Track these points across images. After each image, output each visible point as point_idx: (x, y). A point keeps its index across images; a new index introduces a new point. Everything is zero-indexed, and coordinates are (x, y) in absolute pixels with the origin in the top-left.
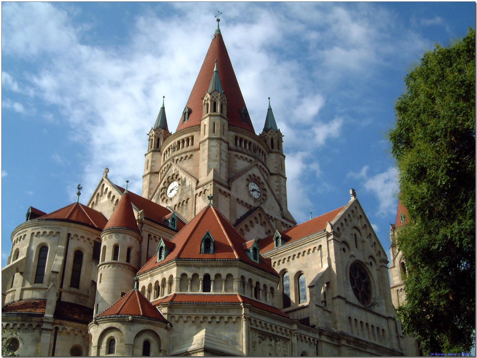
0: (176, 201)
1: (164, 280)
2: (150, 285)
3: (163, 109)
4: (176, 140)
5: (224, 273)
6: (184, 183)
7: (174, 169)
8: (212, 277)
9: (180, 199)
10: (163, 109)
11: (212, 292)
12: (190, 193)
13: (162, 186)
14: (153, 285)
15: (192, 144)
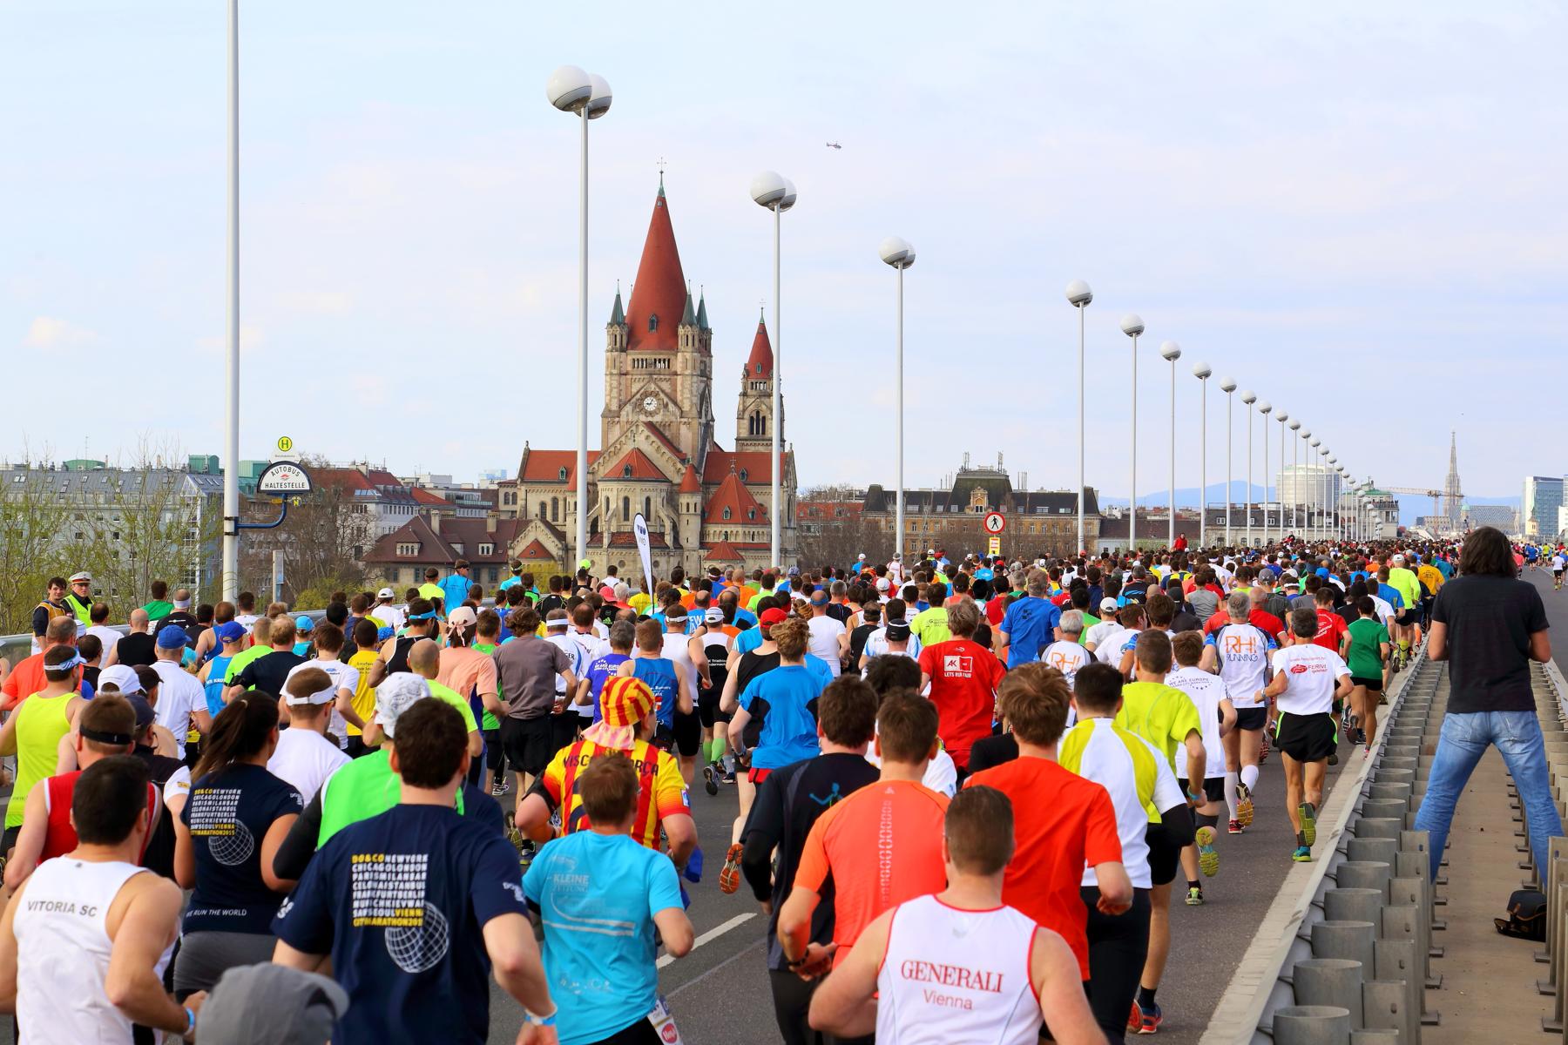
0: (657, 419)
1: (732, 532)
2: (721, 532)
3: (618, 296)
4: (653, 357)
5: (761, 530)
6: (666, 406)
7: (653, 387)
8: (756, 533)
9: (663, 419)
10: (618, 296)
11: (755, 541)
12: (673, 419)
13: (638, 396)
14: (723, 532)
15: (669, 367)
